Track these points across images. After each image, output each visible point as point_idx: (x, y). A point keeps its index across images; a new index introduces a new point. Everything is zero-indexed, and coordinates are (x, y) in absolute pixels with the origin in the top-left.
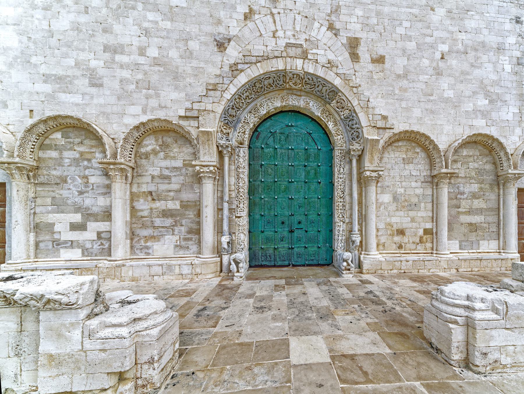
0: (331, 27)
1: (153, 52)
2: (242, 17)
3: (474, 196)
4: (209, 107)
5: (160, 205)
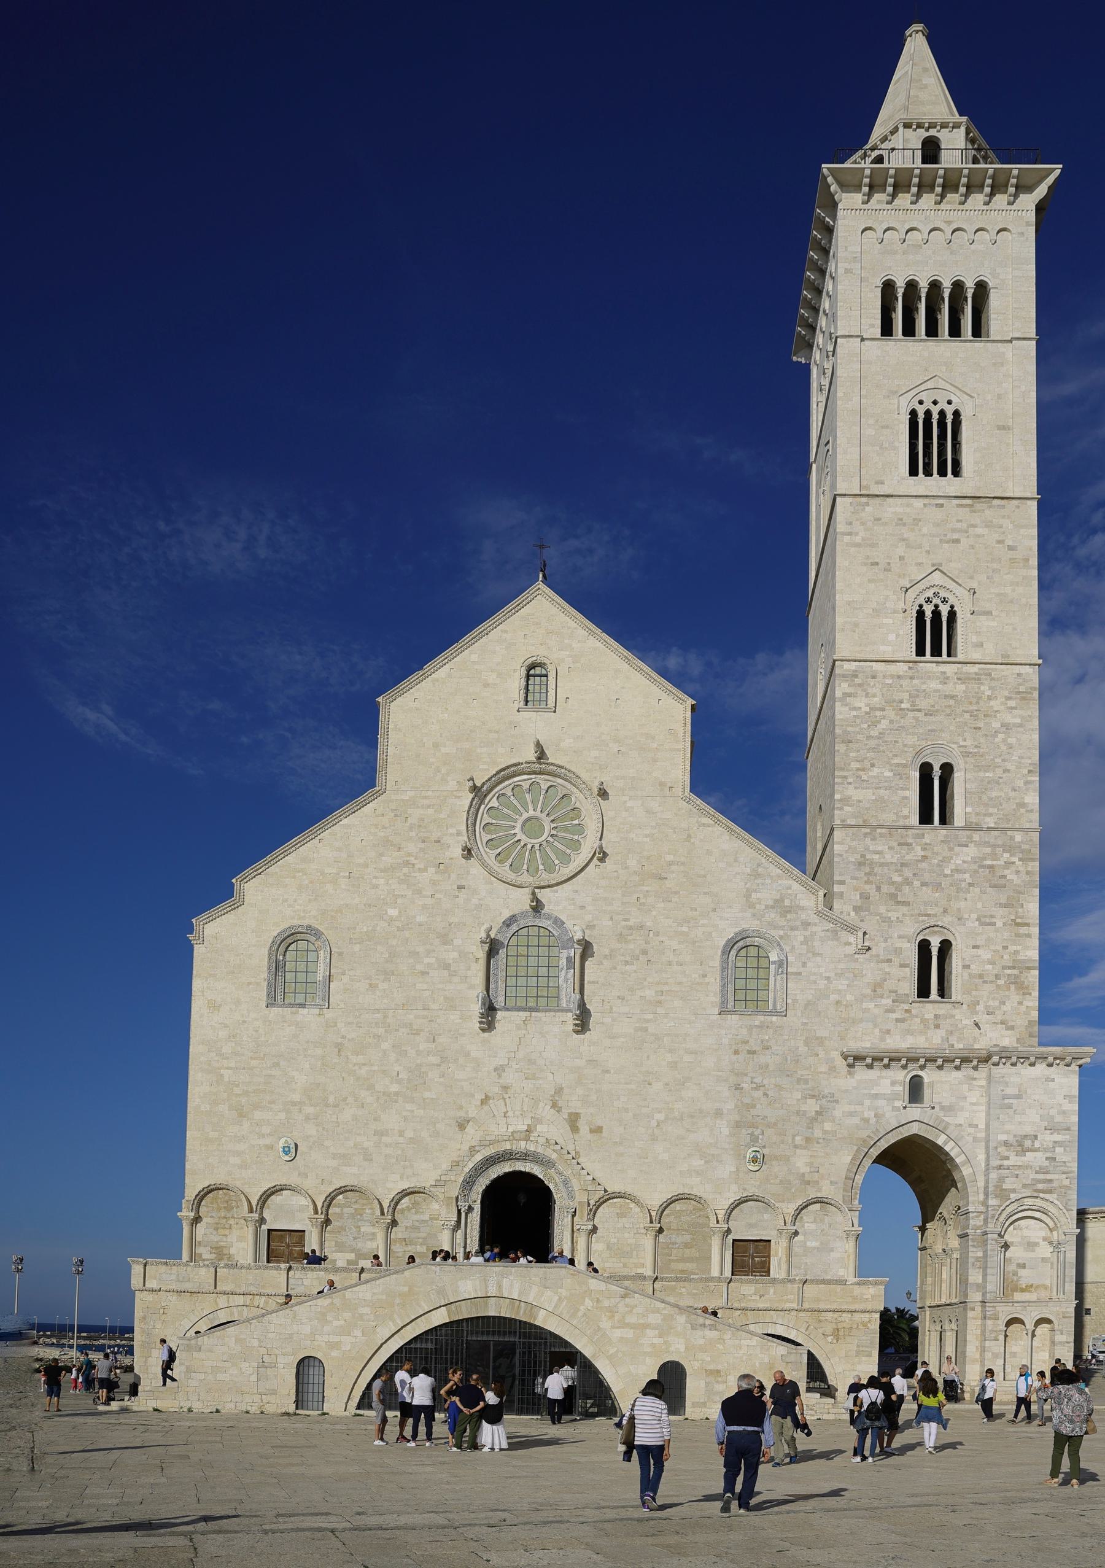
0: (554, 1105)
1: (409, 1134)
3: (687, 1245)
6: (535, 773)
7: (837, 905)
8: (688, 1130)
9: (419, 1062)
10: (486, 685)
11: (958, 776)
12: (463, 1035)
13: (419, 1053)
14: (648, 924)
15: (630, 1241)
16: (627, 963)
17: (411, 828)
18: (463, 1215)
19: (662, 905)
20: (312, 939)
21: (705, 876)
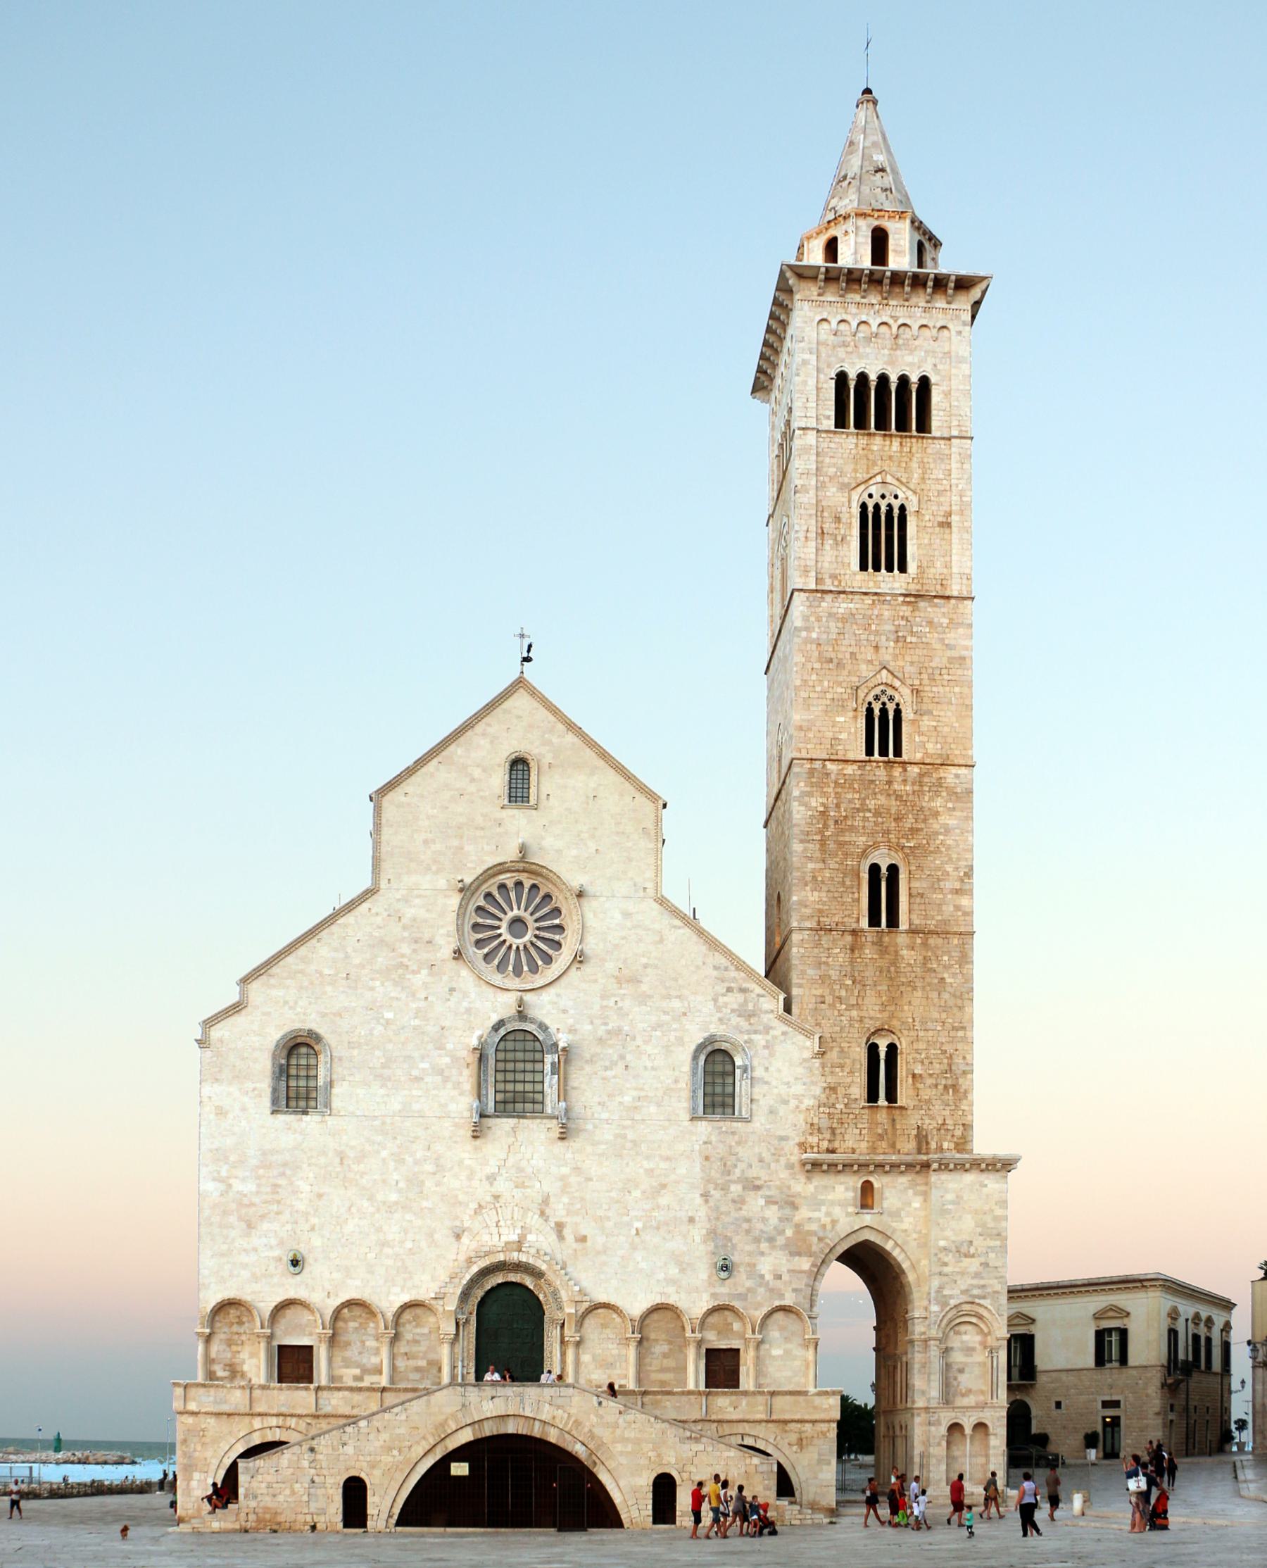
0: (542, 1213)
1: (409, 1245)
2: (472, 1213)
4: (451, 1291)
5: (412, 1363)
6: (518, 871)
7: (795, 1009)
8: (664, 1239)
9: (416, 1170)
10: (473, 780)
11: (903, 877)
12: (456, 1142)
13: (417, 1162)
14: (626, 1028)
15: (615, 1352)
16: (606, 1069)
17: (405, 928)
18: (461, 1328)
19: (637, 1009)
20: (312, 1043)
21: (676, 980)
